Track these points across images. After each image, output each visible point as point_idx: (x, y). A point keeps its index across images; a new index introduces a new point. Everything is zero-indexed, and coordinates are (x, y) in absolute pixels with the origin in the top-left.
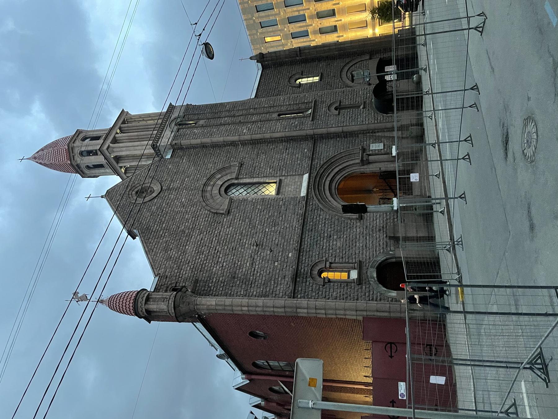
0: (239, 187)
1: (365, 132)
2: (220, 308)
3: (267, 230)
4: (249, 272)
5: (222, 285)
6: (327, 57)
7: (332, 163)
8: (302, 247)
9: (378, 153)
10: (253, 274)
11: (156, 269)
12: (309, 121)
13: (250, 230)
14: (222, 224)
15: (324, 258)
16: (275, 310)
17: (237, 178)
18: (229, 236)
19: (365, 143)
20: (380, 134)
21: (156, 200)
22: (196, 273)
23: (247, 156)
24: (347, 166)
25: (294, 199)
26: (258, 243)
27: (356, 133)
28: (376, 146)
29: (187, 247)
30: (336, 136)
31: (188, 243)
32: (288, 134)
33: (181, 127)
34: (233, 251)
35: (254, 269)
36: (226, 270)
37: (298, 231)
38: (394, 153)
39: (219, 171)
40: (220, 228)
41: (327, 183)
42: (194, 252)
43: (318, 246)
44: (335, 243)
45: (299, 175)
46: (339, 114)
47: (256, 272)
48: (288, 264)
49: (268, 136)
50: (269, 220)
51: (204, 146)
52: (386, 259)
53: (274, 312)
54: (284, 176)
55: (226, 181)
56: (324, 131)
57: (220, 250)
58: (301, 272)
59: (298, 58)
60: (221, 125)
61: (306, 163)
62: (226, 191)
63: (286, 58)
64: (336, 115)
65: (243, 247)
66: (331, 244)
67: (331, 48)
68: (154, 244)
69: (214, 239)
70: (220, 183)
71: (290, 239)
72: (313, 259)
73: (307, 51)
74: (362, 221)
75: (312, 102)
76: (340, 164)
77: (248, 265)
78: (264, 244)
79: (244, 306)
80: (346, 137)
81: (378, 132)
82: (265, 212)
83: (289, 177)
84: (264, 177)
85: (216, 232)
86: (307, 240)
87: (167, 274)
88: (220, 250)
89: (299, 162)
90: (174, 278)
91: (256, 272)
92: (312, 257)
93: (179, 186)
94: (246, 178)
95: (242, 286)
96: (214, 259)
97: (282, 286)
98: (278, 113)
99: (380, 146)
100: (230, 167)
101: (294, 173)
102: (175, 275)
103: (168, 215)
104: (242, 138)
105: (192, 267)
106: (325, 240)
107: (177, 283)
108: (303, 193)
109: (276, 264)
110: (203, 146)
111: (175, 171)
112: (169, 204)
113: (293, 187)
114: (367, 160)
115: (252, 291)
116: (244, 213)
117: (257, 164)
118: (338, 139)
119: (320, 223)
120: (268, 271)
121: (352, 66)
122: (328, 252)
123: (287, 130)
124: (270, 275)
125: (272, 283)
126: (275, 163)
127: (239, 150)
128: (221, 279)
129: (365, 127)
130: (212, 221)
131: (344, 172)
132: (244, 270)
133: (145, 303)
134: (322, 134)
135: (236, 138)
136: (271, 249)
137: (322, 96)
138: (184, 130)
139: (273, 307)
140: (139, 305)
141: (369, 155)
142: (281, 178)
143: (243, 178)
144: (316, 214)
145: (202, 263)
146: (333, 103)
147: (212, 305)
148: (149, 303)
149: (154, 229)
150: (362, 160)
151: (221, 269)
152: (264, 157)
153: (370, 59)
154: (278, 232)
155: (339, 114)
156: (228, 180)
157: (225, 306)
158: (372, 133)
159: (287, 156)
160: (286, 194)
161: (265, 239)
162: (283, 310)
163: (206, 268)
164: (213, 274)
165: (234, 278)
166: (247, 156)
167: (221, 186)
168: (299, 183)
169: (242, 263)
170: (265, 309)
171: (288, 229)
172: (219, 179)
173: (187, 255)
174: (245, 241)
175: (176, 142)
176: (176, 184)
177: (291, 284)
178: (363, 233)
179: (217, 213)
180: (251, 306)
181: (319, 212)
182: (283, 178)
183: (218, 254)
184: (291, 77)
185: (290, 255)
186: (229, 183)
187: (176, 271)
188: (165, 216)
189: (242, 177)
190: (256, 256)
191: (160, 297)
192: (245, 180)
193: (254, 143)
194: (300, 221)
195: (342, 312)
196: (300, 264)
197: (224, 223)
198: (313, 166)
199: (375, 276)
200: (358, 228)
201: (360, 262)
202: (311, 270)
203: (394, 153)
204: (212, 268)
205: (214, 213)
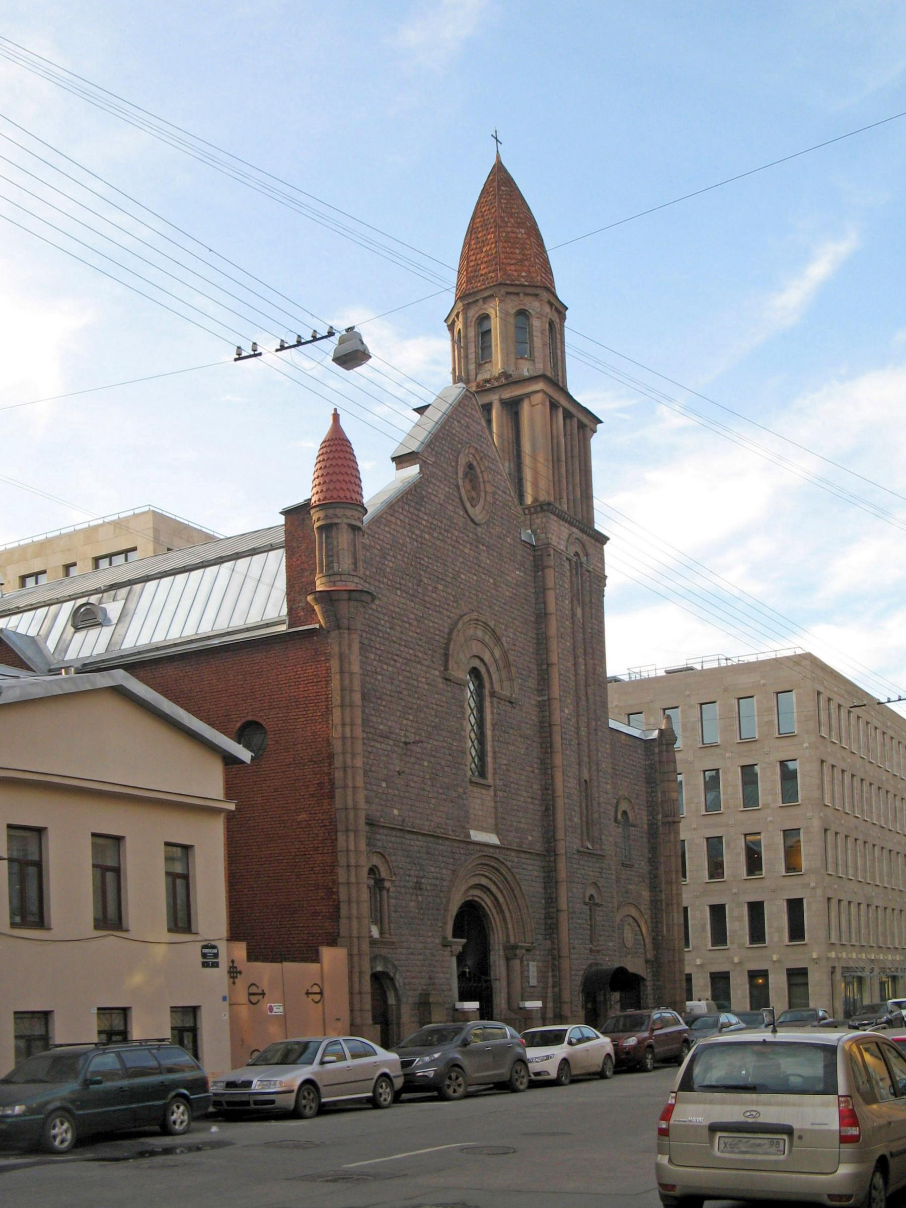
1: (556, 952)
2: (347, 682)
6: (656, 877)
7: (513, 891)
9: (525, 978)
12: (576, 845)
15: (394, 878)
18: (415, 683)
20: (550, 980)
21: (462, 513)
26: (409, 746)
30: (551, 901)
31: (405, 595)
32: (560, 803)
33: (574, 564)
38: (529, 1004)
45: (496, 825)
49: (558, 760)
51: (541, 616)
54: (496, 795)
56: (562, 874)
58: (377, 833)
59: (660, 817)
62: (475, 673)
63: (663, 793)
69: (411, 652)
70: (487, 657)
74: (440, 947)
77: (381, 727)
79: (351, 730)
80: (548, 916)
81: (554, 976)
82: (450, 758)
83: (492, 804)
84: (494, 752)
85: (420, 655)
86: (418, 843)
94: (492, 713)
99: (533, 982)
100: (510, 679)
104: (556, 705)
108: (477, 836)
109: (384, 785)
112: (457, 545)
113: (480, 813)
116: (446, 713)
118: (543, 901)
121: (639, 926)
123: (566, 800)
127: (533, 697)
129: (565, 952)
133: (350, 525)
134: (556, 870)
135: (556, 692)
138: (568, 573)
140: (349, 513)
141: (522, 961)
143: (492, 707)
146: (599, 892)
147: (350, 663)
150: (515, 947)
153: (647, 961)
162: (350, 804)
167: (482, 660)
170: (349, 771)
174: (411, 717)
180: (352, 743)
181: (451, 867)
182: (492, 793)
184: (631, 802)
185: (396, 812)
190: (391, 742)
193: (545, 728)
195: (354, 912)
198: (508, 853)
202: (379, 852)
203: (529, 1004)
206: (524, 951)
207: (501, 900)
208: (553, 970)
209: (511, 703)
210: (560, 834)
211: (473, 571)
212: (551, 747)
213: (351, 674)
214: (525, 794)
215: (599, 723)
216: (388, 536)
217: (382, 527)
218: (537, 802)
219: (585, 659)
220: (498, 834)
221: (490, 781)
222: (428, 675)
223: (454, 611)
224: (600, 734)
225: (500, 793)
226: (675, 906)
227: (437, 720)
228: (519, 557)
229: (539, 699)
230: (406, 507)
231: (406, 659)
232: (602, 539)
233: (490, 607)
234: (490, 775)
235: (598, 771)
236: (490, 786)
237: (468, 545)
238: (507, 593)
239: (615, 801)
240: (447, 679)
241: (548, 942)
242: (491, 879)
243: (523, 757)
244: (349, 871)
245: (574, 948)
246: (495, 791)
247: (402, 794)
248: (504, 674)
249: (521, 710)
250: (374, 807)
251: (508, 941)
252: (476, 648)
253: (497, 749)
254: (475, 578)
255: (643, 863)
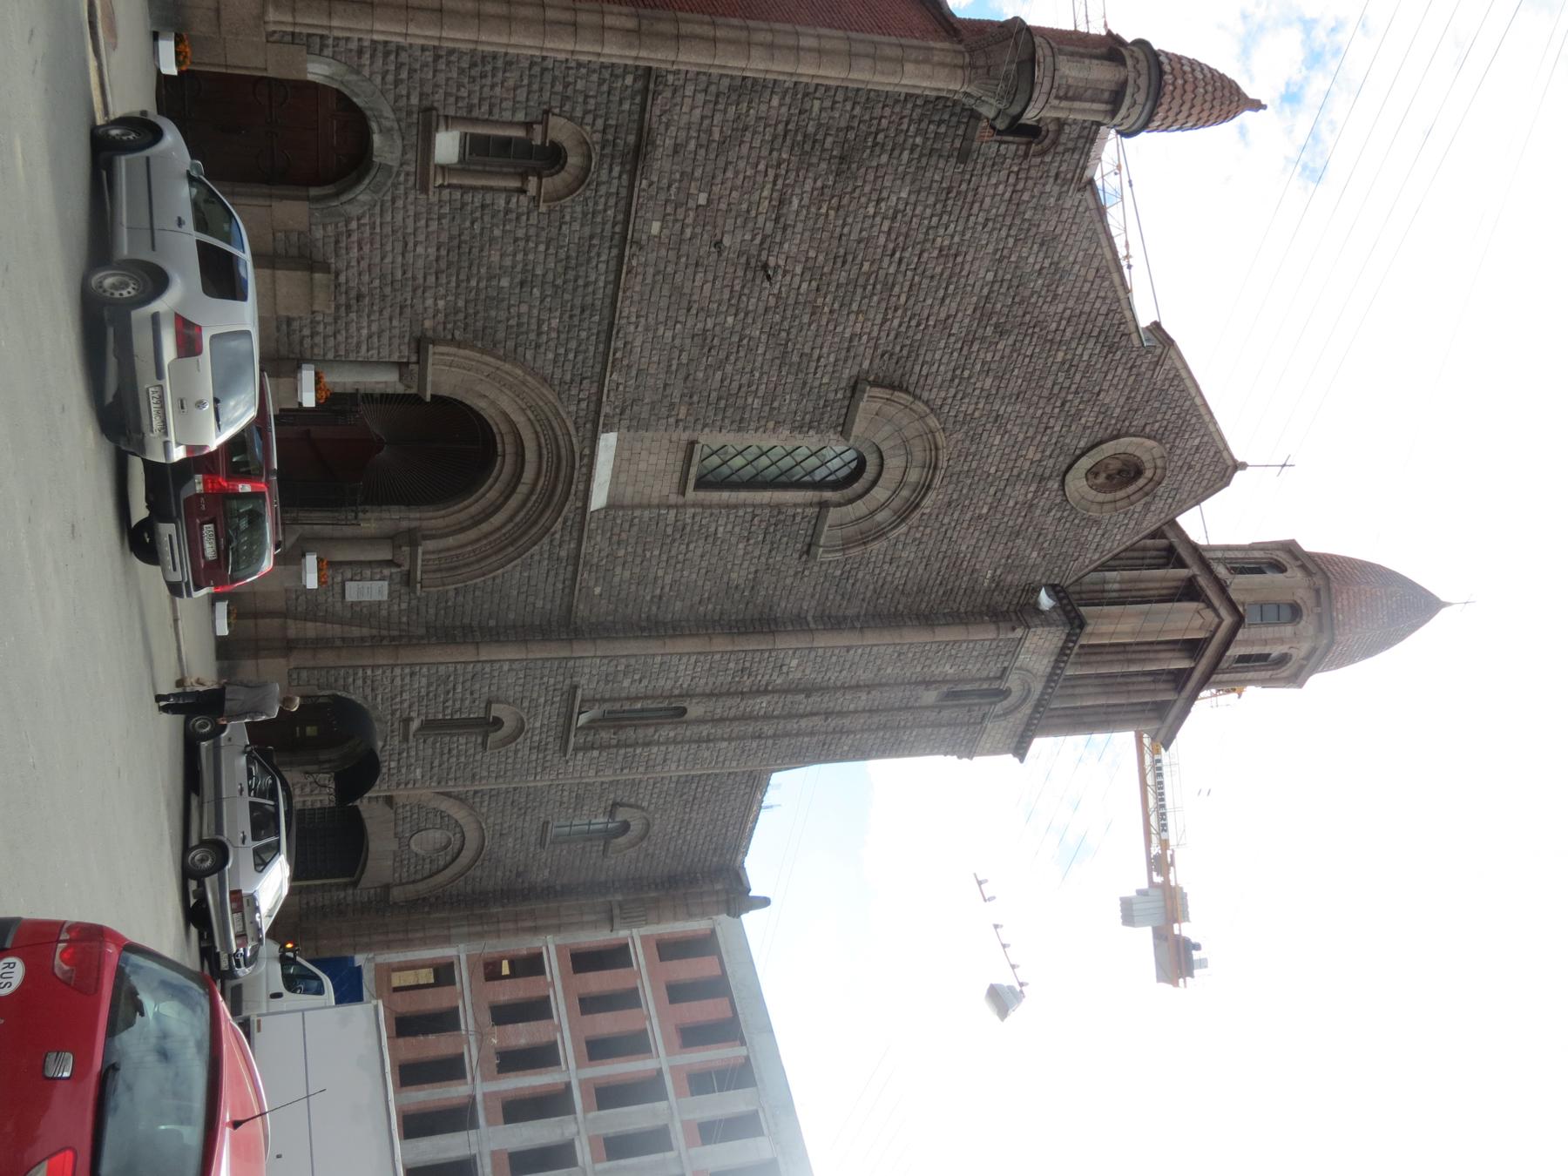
0: (818, 475)
1: (404, 641)
3: (730, 320)
4: (792, 175)
5: (881, 137)
7: (511, 544)
8: (615, 252)
9: (360, 569)
10: (778, 166)
11: (1087, 209)
13: (786, 325)
14: (876, 347)
15: (543, 208)
16: (707, 30)
17: (824, 505)
18: (855, 307)
19: (404, 606)
20: (356, 632)
21: (1082, 444)
22: (964, 187)
23: (788, 581)
24: (463, 530)
25: (638, 425)
26: (761, 274)
27: (433, 640)
28: (370, 591)
29: (990, 276)
31: (985, 291)
33: (995, 685)
34: (842, 251)
35: (775, 183)
36: (867, 189)
37: (627, 309)
39: (880, 533)
40: (883, 334)
41: (528, 474)
42: (969, 258)
43: (562, 254)
44: (508, 262)
45: (622, 507)
46: (489, 703)
47: (771, 172)
48: (662, 196)
50: (722, 355)
52: (337, 195)
53: (714, 24)
54: (669, 507)
55: (860, 497)
56: (538, 652)
57: (887, 259)
58: (622, 164)
59: (619, 897)
60: (869, 687)
61: (595, 546)
62: (861, 462)
64: (498, 701)
65: (810, 264)
66: (520, 257)
67: (511, 926)
68: (1093, 295)
70: (880, 494)
71: (654, 282)
72: (578, 209)
73: (586, 918)
75: (576, 750)
76: (486, 536)
77: (795, 202)
78: (740, 273)
79: (810, 50)
81: (362, 639)
82: (735, 385)
84: (736, 506)
85: (896, 322)
86: (599, 274)
87: (1056, 189)
88: (887, 259)
89: (621, 553)
90: (1033, 173)
91: (771, 172)
92: (585, 214)
93: (1008, 490)
94: (795, 505)
95: (819, 125)
96: (904, 230)
97: (685, 119)
98: (687, 717)
100: (846, 544)
101: (637, 513)
102: (1030, 183)
103: (1046, 393)
104: (801, 642)
105: (977, 205)
106: (539, 271)
107: (1026, 155)
108: (608, 443)
110: (927, 618)
111: (1019, 541)
113: (643, 466)
114: (396, 547)
115: (784, 110)
116: (805, 383)
117: (757, 553)
118: (492, 623)
119: (554, 335)
120: (730, 174)
121: (446, 867)
122: (532, 231)
123: (658, 659)
124: (721, 164)
125: (716, 131)
126: (699, 551)
127: (814, 603)
128: (884, 158)
129: (407, 656)
130: (909, 364)
131: (473, 510)
132: (808, 187)
135: (823, 641)
136: (720, 253)
137: (544, 769)
138: (985, 674)
139: (715, 40)
141: (390, 563)
142: (681, 500)
143: (805, 505)
144: (568, 366)
145: (945, 218)
147: (916, 62)
148: (1113, 87)
149: (1090, 345)
151: (885, 194)
152: (734, 575)
153: (387, 887)
154: (694, 311)
155: (489, 703)
156: (851, 501)
157: (874, 57)
158: (383, 638)
159: (660, 573)
160: (665, 442)
161: (737, 288)
162: (685, 29)
163: (931, 200)
164: (908, 179)
165: (842, 158)
166: (788, 581)
167: (874, 483)
168: (623, 478)
169: (813, 210)
171: (662, 318)
172: (882, 506)
173: (990, 249)
174: (805, 286)
175: (1011, 635)
176: (1019, 493)
177: (655, 126)
178: (414, 290)
179: (892, 387)
180: (789, 48)
182: (673, 499)
183: (891, 246)
184: (642, 839)
185: (656, 227)
186: (849, 492)
187: (1026, 197)
188: (1056, 391)
189: (809, 511)
191: (1077, 105)
192: (799, 500)
194: (620, 344)
196: (624, 193)
197: (869, 352)
198: (575, 534)
199: (377, 139)
200: (431, 312)
201: (424, 189)
204: (913, 199)
205: (900, 388)
206: (406, 568)
207: (498, 519)
208: (373, 637)
209: (808, 552)
210: (604, 648)
211: (1002, 466)
212: (740, 634)
213: (901, 61)
214: (668, 580)
215: (770, 742)
216: (1071, 259)
217: (1085, 244)
218: (654, 608)
219: (864, 711)
220: (609, 506)
221: (691, 494)
222: (865, 338)
223: (952, 413)
224: (755, 745)
225: (673, 512)
226: (479, 928)
227: (795, 359)
228: (1009, 578)
229: (810, 618)
230: (1104, 310)
231: (893, 285)
232: (1020, 750)
233: (949, 504)
234: (703, 495)
235: (699, 741)
236: (683, 494)
237: (1038, 456)
238: (964, 548)
239: (645, 804)
240: (854, 389)
241: (422, 631)
242: (531, 492)
243: (725, 579)
244: (567, 9)
245: (412, 674)
246: (676, 506)
247: (685, 247)
248: (851, 531)
249: (796, 573)
250: (667, 165)
251: (426, 538)
252: (894, 463)
253: (741, 513)
254: (993, 470)
255: (546, 872)
